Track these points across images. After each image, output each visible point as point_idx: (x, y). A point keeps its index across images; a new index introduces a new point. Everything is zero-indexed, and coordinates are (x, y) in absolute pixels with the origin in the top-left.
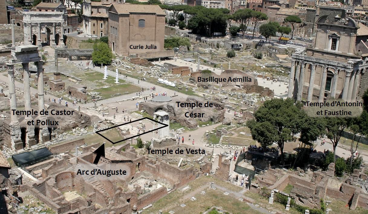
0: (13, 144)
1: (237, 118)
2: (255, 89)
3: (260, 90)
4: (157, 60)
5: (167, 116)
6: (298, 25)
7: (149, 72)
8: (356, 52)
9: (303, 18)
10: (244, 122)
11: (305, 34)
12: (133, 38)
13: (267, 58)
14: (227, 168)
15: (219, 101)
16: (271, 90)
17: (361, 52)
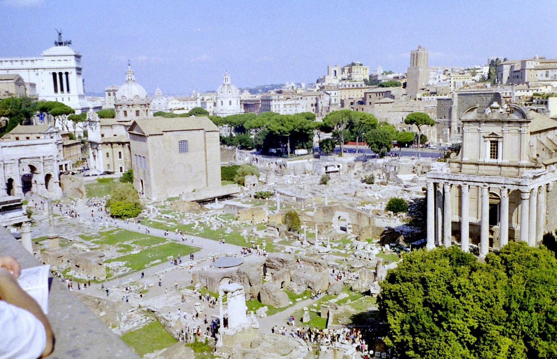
4: (213, 200)
7: (203, 221)
9: (433, 114)
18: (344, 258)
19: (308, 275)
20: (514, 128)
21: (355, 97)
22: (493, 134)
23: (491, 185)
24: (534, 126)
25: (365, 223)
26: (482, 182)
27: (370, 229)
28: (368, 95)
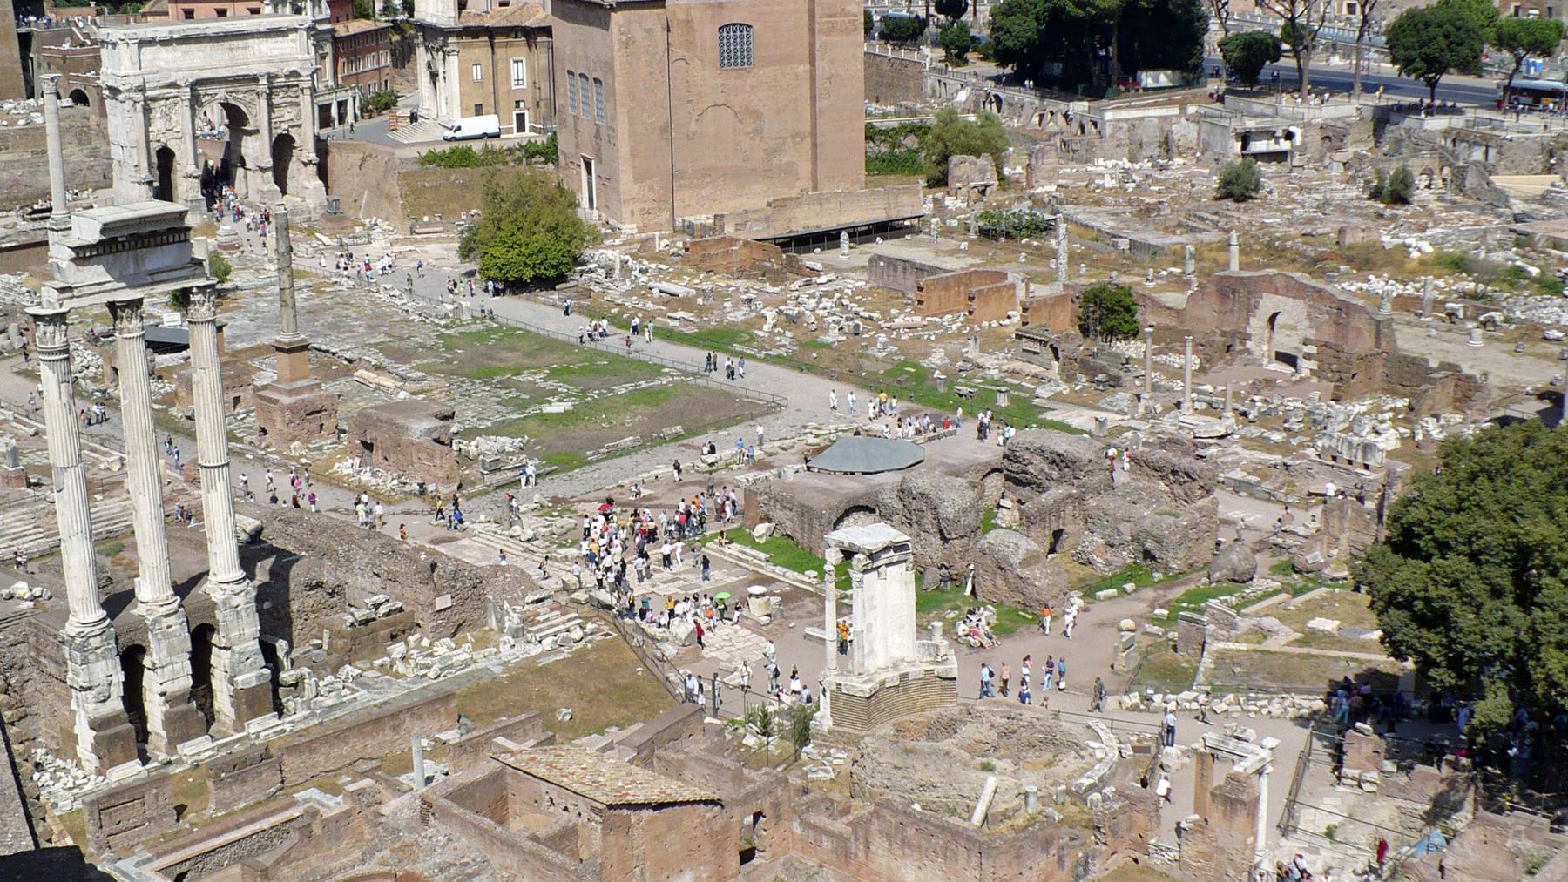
0: (86, 737)
1: (1290, 541)
2: (1380, 372)
3: (1409, 377)
4: (828, 239)
5: (900, 547)
7: (792, 310)
10: (1326, 564)
12: (693, 127)
13: (1440, 199)
14: (1241, 819)
15: (1186, 453)
16: (1470, 378)
18: (1277, 458)
19: (1147, 514)
25: (1363, 344)
27: (1379, 362)
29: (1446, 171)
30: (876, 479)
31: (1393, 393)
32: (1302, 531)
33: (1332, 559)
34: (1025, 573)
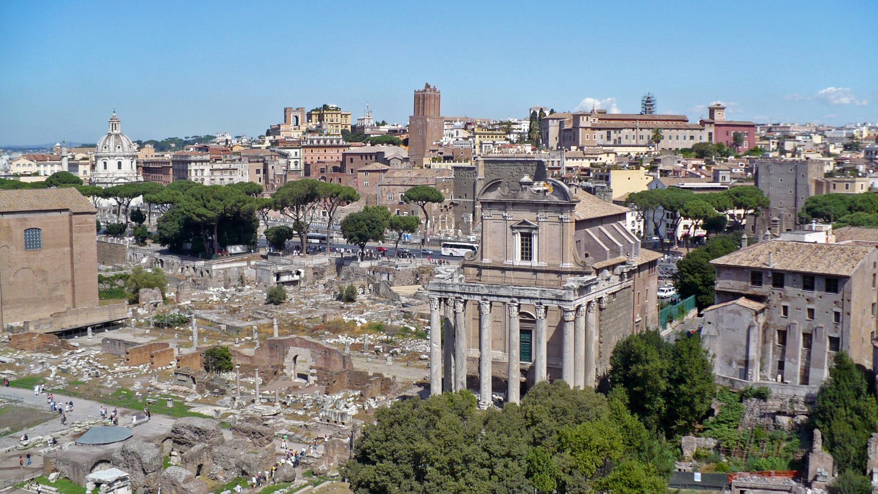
1: (310, 461)
2: (346, 380)
3: (360, 381)
5: (123, 479)
6: (435, 206)
7: (64, 366)
8: (580, 260)
9: (447, 190)
10: (328, 470)
11: (457, 227)
13: (369, 298)
15: (259, 424)
16: (388, 379)
17: (591, 258)
18: (302, 423)
19: (242, 453)
20: (552, 216)
21: (329, 159)
22: (524, 222)
23: (522, 302)
24: (582, 212)
25: (338, 367)
26: (509, 297)
27: (346, 375)
28: (348, 158)
29: (371, 286)
30: (110, 446)
31: (354, 389)
32: (316, 456)
33: (330, 467)
34: (186, 486)
